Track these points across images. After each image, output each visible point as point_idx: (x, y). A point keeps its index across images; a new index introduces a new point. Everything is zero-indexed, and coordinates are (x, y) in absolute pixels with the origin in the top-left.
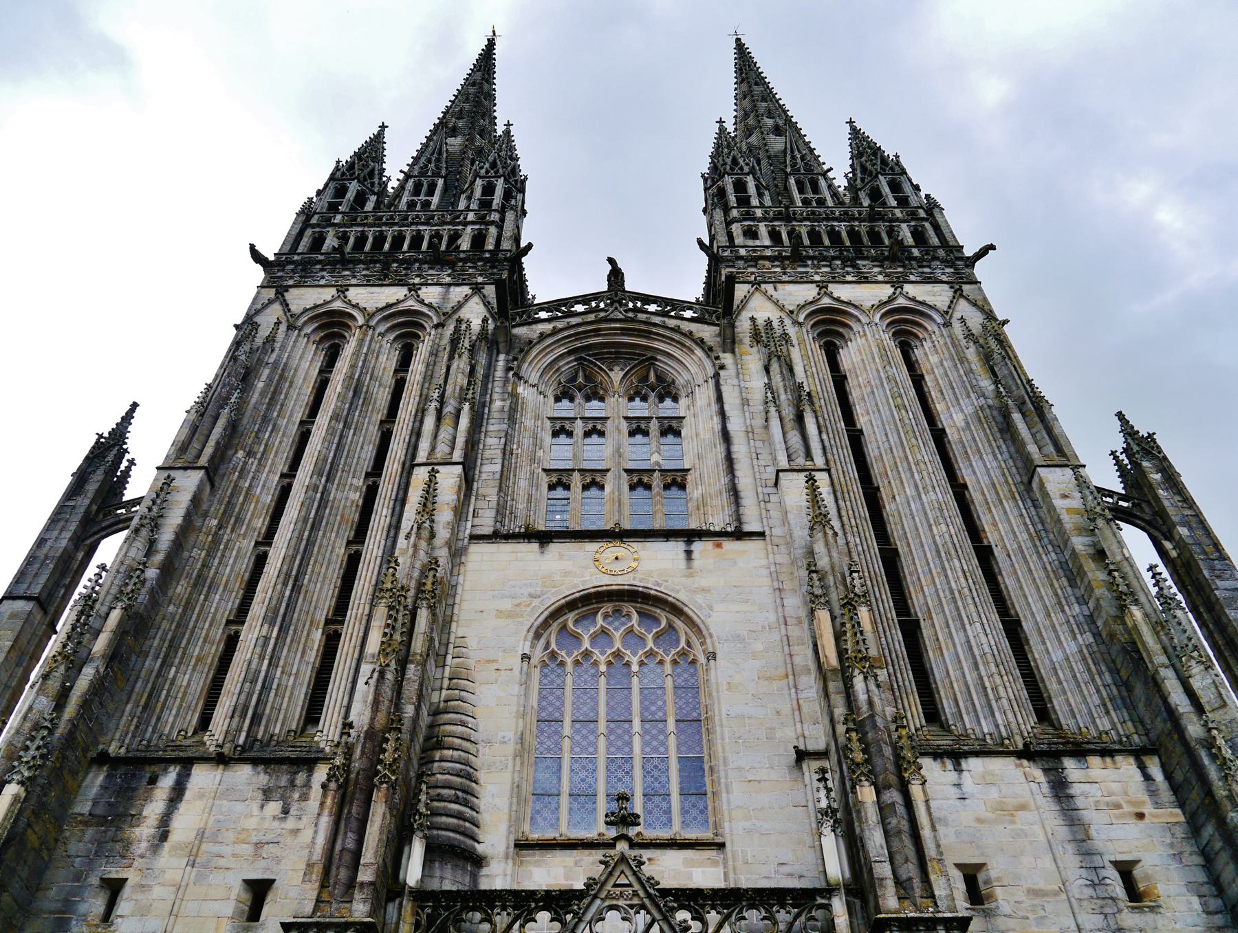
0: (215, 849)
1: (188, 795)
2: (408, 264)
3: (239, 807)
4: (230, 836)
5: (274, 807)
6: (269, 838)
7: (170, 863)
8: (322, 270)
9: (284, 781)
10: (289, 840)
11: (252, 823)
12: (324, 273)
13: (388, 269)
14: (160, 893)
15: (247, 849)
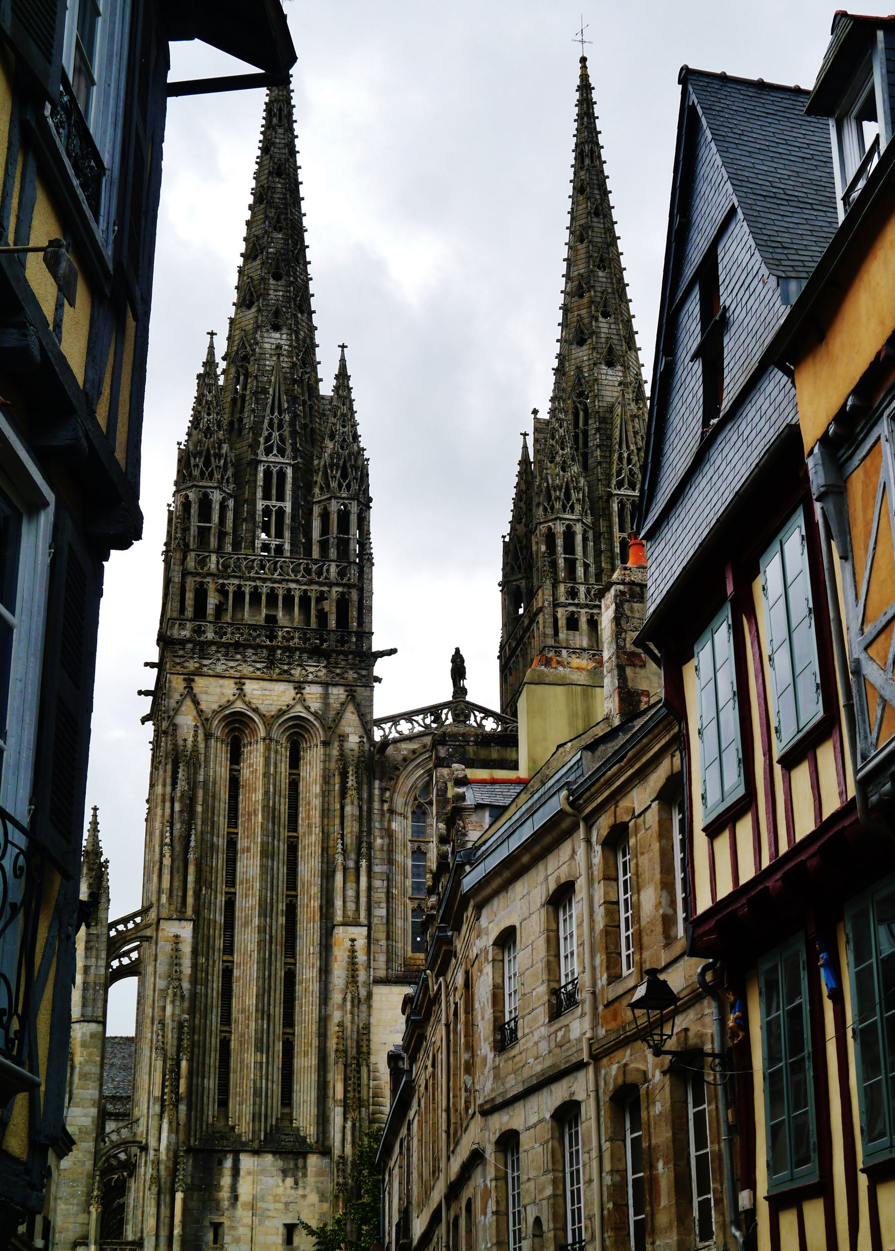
0: (265, 1205)
1: (242, 1173)
2: (290, 652)
3: (271, 1181)
4: (270, 1198)
5: (290, 1181)
6: (291, 1199)
7: (243, 1214)
8: (217, 652)
9: (292, 1166)
10: (301, 1201)
11: (280, 1191)
12: (219, 655)
13: (273, 656)
14: (243, 1231)
15: (280, 1206)
